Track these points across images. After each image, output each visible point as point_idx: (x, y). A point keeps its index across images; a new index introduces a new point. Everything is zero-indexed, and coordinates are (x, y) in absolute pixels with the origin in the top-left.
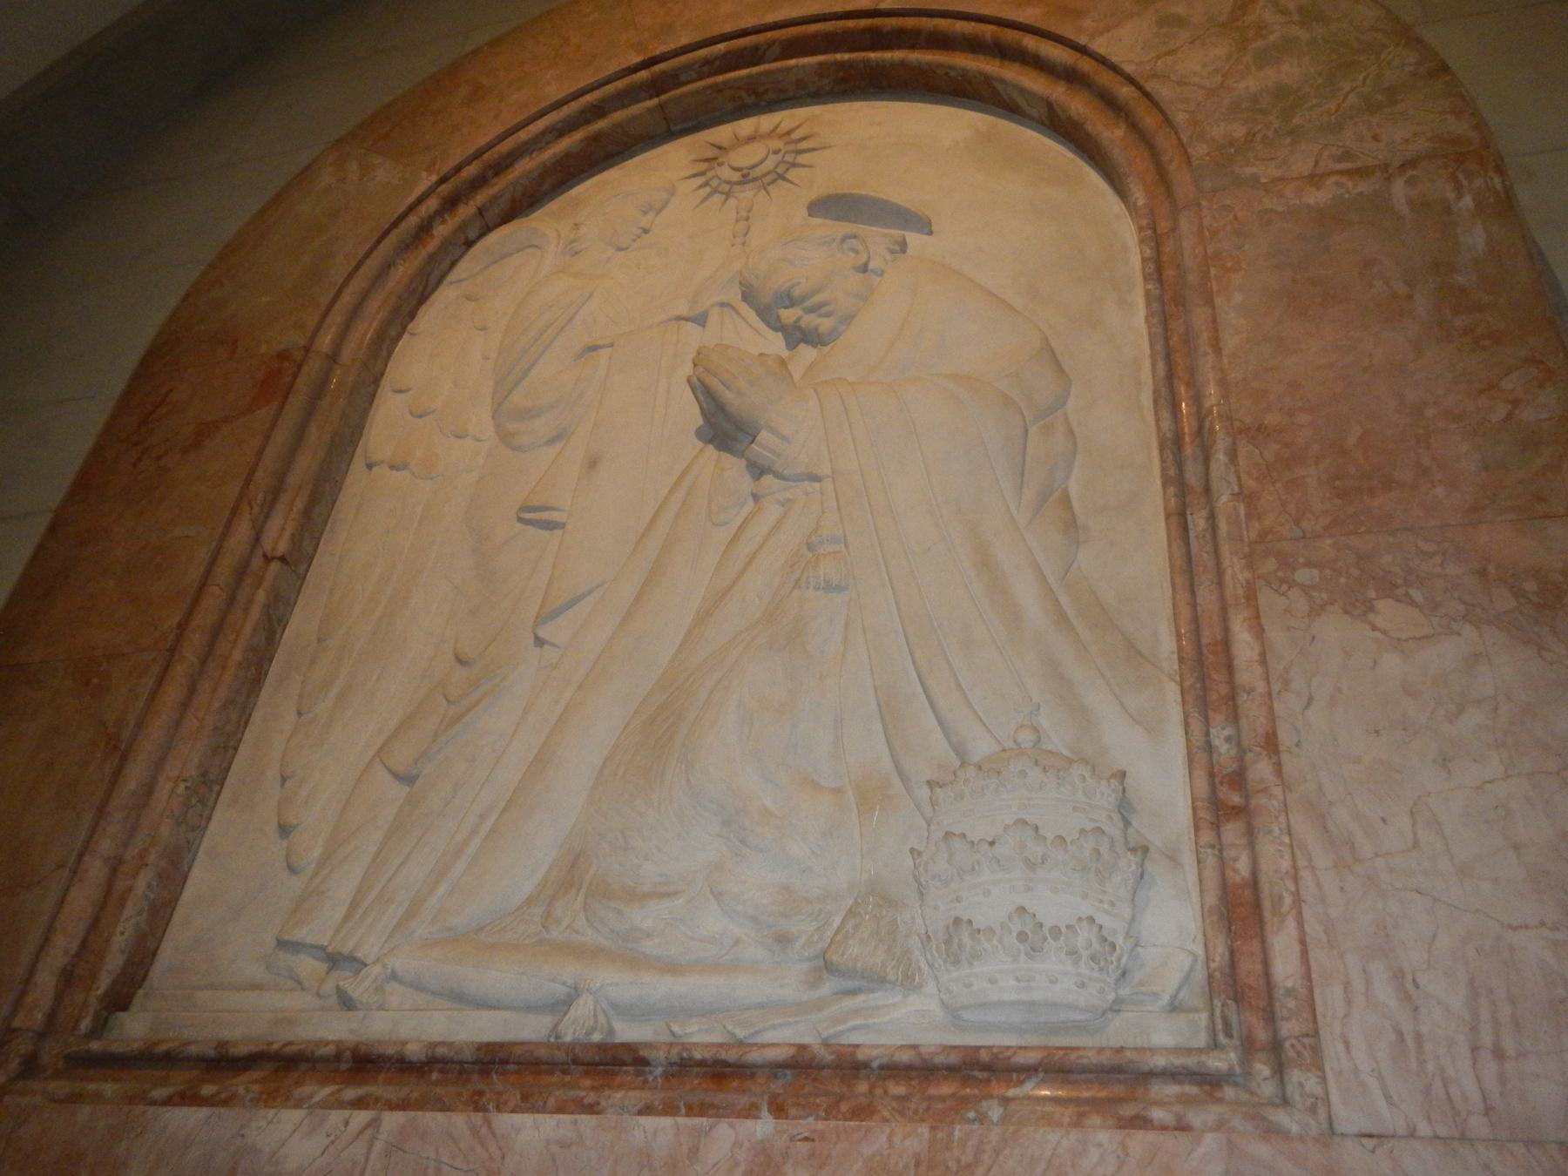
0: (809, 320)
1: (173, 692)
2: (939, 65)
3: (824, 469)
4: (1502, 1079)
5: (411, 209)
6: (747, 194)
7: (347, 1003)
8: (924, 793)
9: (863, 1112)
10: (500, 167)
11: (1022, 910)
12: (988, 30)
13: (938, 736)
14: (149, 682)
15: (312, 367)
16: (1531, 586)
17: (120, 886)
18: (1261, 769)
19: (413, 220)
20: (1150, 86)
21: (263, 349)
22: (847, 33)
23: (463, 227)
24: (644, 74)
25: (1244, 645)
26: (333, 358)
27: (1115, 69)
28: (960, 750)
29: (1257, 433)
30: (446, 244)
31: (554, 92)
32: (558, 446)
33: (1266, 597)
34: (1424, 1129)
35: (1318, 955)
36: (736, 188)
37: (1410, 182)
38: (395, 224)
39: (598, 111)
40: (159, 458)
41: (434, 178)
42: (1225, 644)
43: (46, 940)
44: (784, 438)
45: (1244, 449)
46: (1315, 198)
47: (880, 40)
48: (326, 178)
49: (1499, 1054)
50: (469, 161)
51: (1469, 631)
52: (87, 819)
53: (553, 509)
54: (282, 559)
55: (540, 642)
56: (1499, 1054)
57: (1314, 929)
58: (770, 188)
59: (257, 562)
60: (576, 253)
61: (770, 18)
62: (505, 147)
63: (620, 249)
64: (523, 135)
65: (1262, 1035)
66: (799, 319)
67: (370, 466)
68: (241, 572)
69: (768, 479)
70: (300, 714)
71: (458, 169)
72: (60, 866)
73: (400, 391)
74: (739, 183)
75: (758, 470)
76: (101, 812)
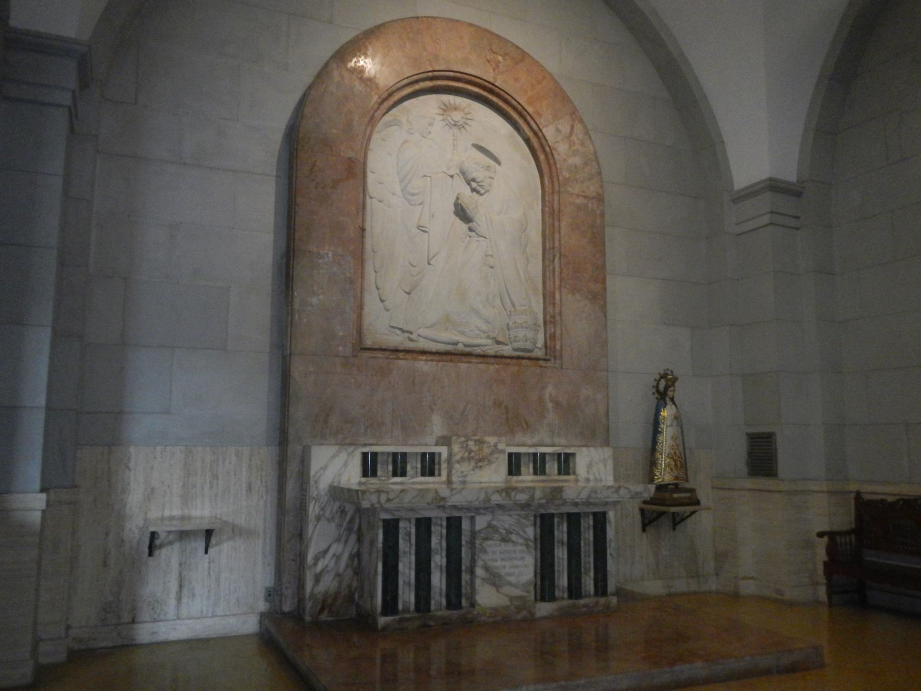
0: (478, 188)
3: (487, 237)
6: (455, 130)
7: (411, 340)
8: (509, 313)
9: (508, 364)
11: (525, 336)
13: (509, 302)
18: (558, 318)
20: (553, 152)
25: (557, 296)
28: (513, 305)
29: (565, 256)
32: (422, 206)
33: (562, 289)
35: (563, 346)
36: (452, 126)
37: (592, 203)
39: (417, 82)
42: (554, 294)
44: (479, 225)
46: (578, 201)
47: (491, 92)
53: (424, 227)
55: (429, 264)
58: (461, 129)
61: (467, 71)
63: (424, 137)
65: (552, 354)
66: (476, 187)
67: (371, 198)
69: (473, 234)
70: (376, 272)
74: (453, 125)
75: (470, 230)
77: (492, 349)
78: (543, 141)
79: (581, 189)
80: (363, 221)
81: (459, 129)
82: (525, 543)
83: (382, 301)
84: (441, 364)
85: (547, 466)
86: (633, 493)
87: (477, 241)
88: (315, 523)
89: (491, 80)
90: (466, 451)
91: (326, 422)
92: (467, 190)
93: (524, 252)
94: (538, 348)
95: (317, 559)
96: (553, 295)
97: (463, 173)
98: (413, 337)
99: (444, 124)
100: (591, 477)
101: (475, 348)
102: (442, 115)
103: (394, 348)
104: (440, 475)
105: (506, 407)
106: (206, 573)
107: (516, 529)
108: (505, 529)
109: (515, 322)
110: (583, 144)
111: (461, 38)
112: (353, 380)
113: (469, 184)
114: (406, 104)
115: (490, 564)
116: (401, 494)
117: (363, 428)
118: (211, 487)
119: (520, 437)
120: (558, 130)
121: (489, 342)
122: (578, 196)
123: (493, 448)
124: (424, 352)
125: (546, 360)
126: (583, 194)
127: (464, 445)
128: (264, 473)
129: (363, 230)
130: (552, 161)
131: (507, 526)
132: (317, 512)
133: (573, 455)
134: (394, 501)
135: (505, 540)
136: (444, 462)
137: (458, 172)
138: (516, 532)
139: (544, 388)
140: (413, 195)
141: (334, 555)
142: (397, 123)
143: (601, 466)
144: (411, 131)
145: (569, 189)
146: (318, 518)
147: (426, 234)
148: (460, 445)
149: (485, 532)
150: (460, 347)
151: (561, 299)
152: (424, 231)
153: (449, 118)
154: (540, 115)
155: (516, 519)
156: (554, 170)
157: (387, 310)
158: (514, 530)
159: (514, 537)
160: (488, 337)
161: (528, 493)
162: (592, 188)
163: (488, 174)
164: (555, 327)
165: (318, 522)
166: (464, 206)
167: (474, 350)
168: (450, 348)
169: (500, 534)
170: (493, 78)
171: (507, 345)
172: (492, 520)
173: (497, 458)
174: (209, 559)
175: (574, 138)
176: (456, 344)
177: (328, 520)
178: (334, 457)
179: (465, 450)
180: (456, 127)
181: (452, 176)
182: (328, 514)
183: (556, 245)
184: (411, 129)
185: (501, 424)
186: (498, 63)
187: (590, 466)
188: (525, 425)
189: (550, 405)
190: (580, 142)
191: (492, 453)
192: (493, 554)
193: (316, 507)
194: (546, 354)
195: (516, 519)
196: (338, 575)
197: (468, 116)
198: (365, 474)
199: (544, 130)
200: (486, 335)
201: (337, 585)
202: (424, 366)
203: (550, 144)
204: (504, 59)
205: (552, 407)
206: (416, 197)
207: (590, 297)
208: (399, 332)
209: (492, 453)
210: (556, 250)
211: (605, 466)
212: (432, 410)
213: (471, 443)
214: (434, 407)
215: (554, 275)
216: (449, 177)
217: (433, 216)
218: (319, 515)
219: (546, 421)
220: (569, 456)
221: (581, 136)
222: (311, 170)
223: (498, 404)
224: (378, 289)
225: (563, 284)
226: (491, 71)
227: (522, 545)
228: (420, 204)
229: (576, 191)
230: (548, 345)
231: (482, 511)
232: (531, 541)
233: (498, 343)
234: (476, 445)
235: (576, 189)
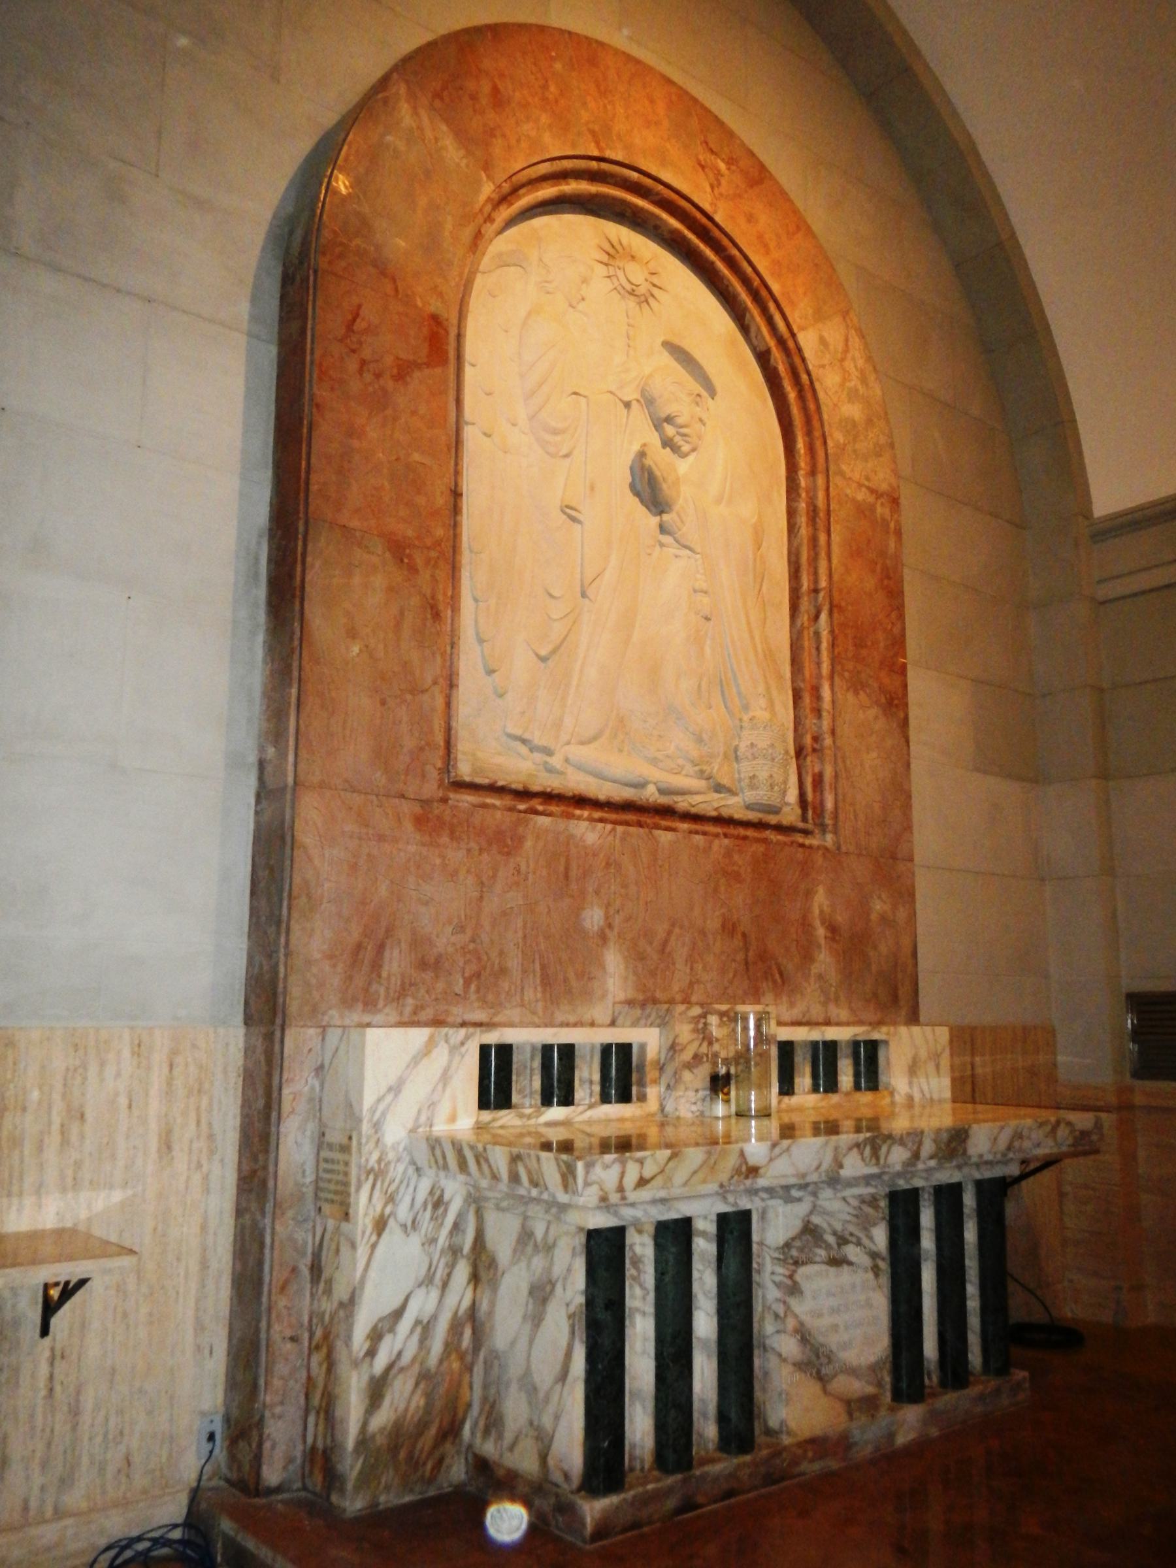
0: (677, 439)
2: (728, 280)
6: (631, 303)
7: (550, 770)
12: (756, 282)
18: (828, 741)
22: (695, 220)
24: (594, 165)
25: (826, 692)
27: (803, 360)
29: (840, 607)
33: (837, 679)
35: (841, 804)
39: (563, 176)
40: (378, 376)
45: (836, 615)
47: (704, 234)
53: (575, 510)
57: (840, 797)
60: (548, 293)
70: (476, 600)
75: (663, 529)
77: (707, 802)
78: (797, 360)
80: (457, 473)
81: (639, 303)
84: (620, 829)
87: (676, 556)
88: (374, 1238)
89: (706, 207)
90: (704, 1039)
91: (376, 966)
92: (654, 439)
95: (376, 1337)
96: (816, 691)
97: (649, 402)
98: (556, 761)
99: (612, 287)
100: (917, 1096)
101: (678, 798)
103: (520, 787)
104: (642, 1098)
105: (744, 935)
106: (43, 1393)
108: (835, 1233)
109: (752, 745)
110: (864, 380)
111: (652, 101)
112: (438, 861)
113: (658, 426)
116: (671, 1164)
117: (461, 981)
118: (65, 1142)
124: (581, 801)
125: (806, 832)
127: (701, 1026)
128: (205, 1102)
129: (456, 494)
130: (812, 406)
131: (839, 1227)
132: (379, 1209)
133: (886, 1042)
134: (653, 1183)
135: (837, 1262)
137: (637, 395)
139: (809, 894)
140: (555, 432)
141: (418, 1322)
144: (546, 285)
145: (844, 467)
146: (380, 1225)
147: (579, 526)
148: (692, 1026)
150: (650, 794)
151: (833, 702)
152: (574, 519)
153: (620, 274)
154: (792, 303)
155: (855, 1208)
156: (816, 423)
158: (851, 1234)
159: (851, 1251)
160: (701, 774)
162: (881, 475)
164: (822, 761)
165: (379, 1235)
166: (658, 473)
167: (676, 802)
168: (628, 794)
169: (828, 1247)
170: (711, 204)
172: (811, 1213)
174: (52, 1350)
175: (849, 365)
176: (641, 785)
177: (404, 1226)
178: (416, 1060)
179: (701, 1036)
180: (632, 298)
181: (627, 405)
182: (403, 1212)
183: (823, 583)
184: (546, 282)
186: (718, 174)
188: (777, 976)
189: (821, 932)
192: (814, 1298)
193: (377, 1193)
194: (804, 819)
195: (855, 1208)
196: (425, 1376)
197: (655, 280)
198: (484, 1103)
199: (802, 337)
200: (697, 768)
201: (422, 1403)
203: (811, 367)
204: (729, 169)
206: (558, 438)
207: (883, 700)
208: (524, 750)
210: (821, 594)
211: (938, 1067)
213: (713, 1020)
215: (818, 649)
216: (622, 405)
217: (592, 488)
218: (382, 1215)
220: (873, 1047)
221: (861, 363)
222: (350, 327)
223: (729, 928)
224: (481, 641)
225: (838, 668)
228: (566, 456)
230: (810, 796)
231: (795, 1193)
232: (883, 1259)
233: (718, 788)
234: (721, 1025)
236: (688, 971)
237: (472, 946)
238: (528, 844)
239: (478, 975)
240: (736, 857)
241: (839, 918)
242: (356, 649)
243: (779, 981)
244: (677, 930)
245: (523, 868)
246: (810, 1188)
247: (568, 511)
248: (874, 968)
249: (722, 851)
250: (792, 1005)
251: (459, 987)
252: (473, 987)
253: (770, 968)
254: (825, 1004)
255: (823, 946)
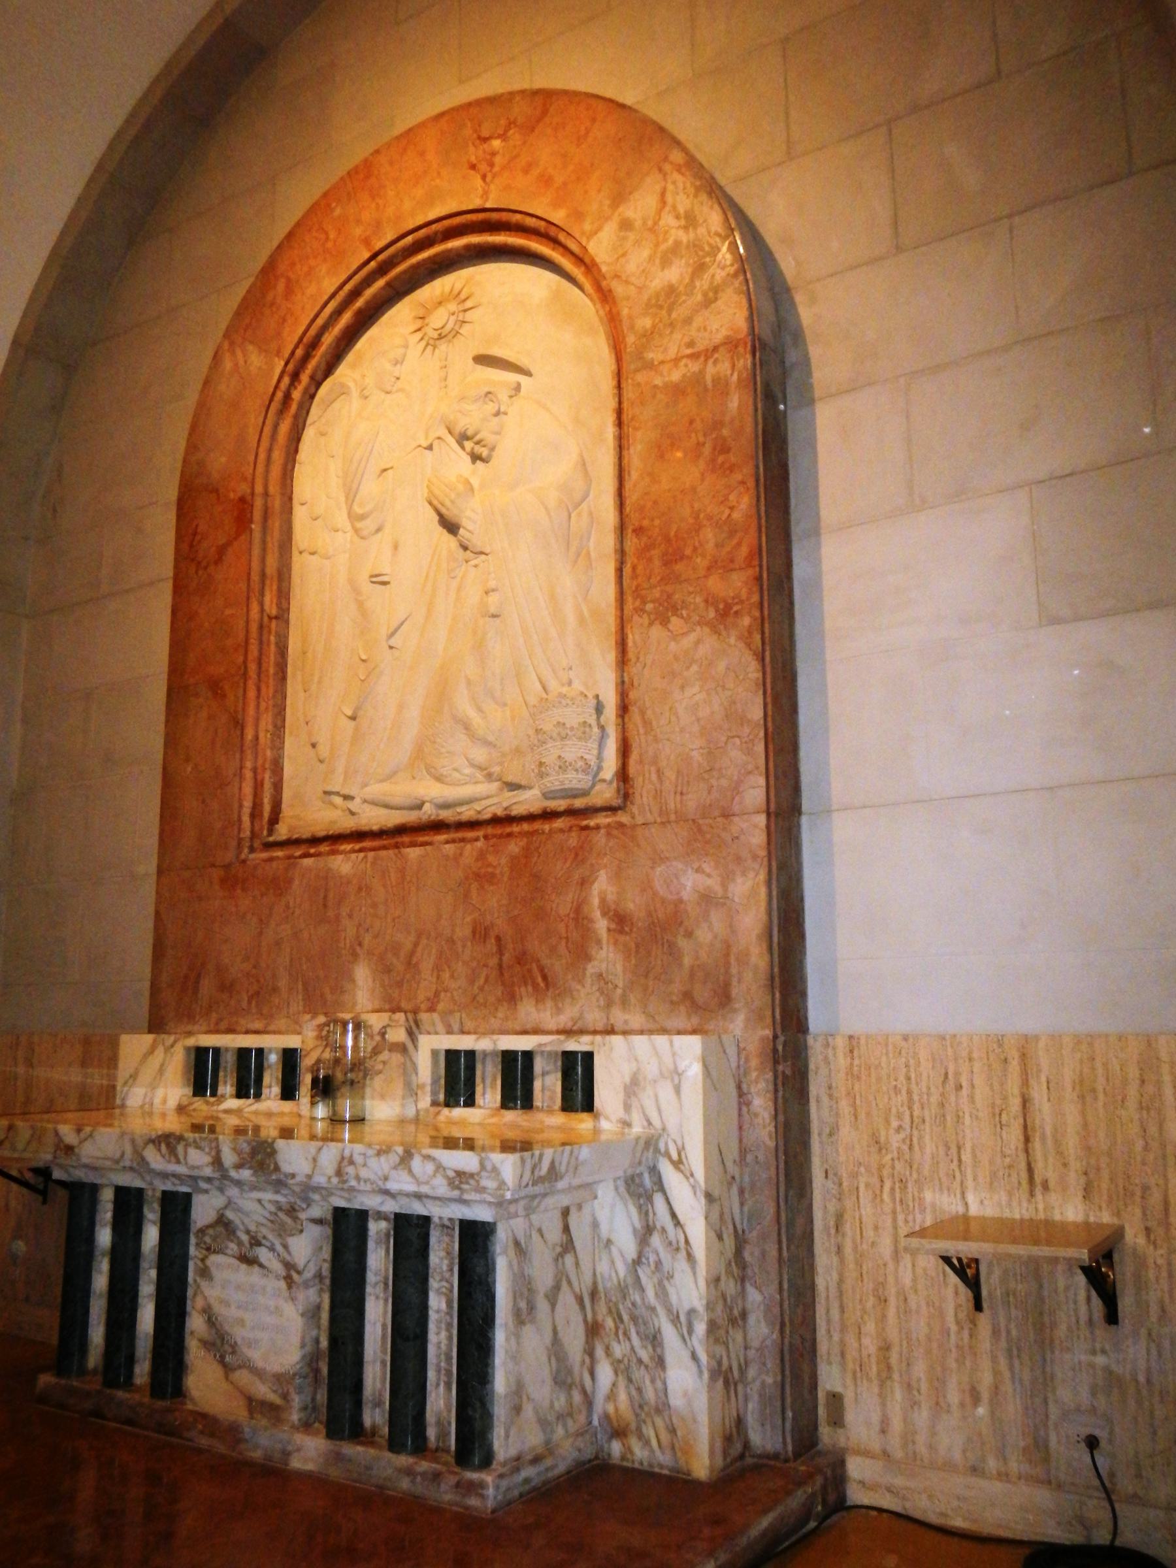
0: (479, 450)
1: (252, 693)
3: (487, 551)
4: (681, 802)
5: (277, 387)
10: (314, 344)
11: (560, 757)
14: (241, 691)
15: (258, 503)
16: (721, 606)
17: (259, 778)
19: (280, 395)
21: (232, 495)
23: (306, 389)
24: (373, 264)
26: (266, 494)
30: (301, 405)
31: (330, 285)
32: (380, 535)
34: (659, 820)
38: (271, 401)
39: (356, 293)
41: (282, 363)
43: (241, 806)
46: (676, 376)
48: (228, 365)
49: (682, 794)
50: (296, 347)
51: (698, 628)
52: (238, 756)
54: (276, 618)
55: (391, 647)
56: (682, 794)
59: (266, 619)
61: (432, 216)
62: (313, 332)
63: (387, 393)
64: (320, 321)
67: (301, 553)
68: (261, 627)
71: (293, 353)
72: (235, 775)
73: (302, 504)
76: (242, 751)
77: (495, 802)
79: (686, 339)
82: (283, 1272)
83: (314, 746)
85: (537, 1085)
86: (451, 1174)
89: (477, 203)
90: (326, 1046)
91: (196, 991)
93: (578, 555)
94: (604, 781)
101: (459, 810)
102: (419, 330)
105: (498, 939)
107: (270, 1236)
108: (248, 1232)
112: (234, 909)
114: (362, 344)
115: (217, 1308)
119: (528, 1011)
120: (626, 225)
121: (495, 786)
122: (676, 361)
123: (378, 1038)
124: (359, 836)
126: (689, 351)
127: (324, 1033)
135: (249, 1260)
136: (308, 1070)
137: (443, 432)
138: (268, 1244)
139: (584, 883)
142: (344, 391)
143: (666, 1092)
149: (211, 1231)
150: (429, 812)
155: (271, 1213)
157: (321, 761)
159: (263, 1254)
160: (489, 777)
161: (207, 1150)
163: (491, 407)
168: (410, 817)
169: (240, 1244)
171: (530, 788)
172: (226, 1207)
173: (384, 1063)
176: (419, 807)
185: (486, 980)
187: (632, 1088)
188: (539, 980)
189: (602, 925)
190: (683, 222)
191: (376, 1051)
192: (223, 1288)
195: (271, 1213)
197: (469, 304)
202: (344, 864)
205: (609, 930)
207: (712, 614)
209: (376, 1051)
212: (355, 955)
214: (358, 948)
219: (591, 969)
223: (480, 933)
226: (478, 182)
227: (277, 1277)
229: (672, 353)
233: (514, 787)
235: (674, 344)
236: (434, 980)
237: (254, 971)
238: (297, 882)
239: (258, 993)
240: (491, 858)
241: (631, 906)
242: (189, 769)
243: (542, 985)
244: (424, 941)
245: (291, 904)
246: (217, 1183)
247: (374, 579)
248: (687, 961)
249: (475, 854)
250: (559, 1011)
251: (244, 1004)
252: (254, 1003)
253: (530, 971)
254: (609, 1005)
255: (604, 941)
